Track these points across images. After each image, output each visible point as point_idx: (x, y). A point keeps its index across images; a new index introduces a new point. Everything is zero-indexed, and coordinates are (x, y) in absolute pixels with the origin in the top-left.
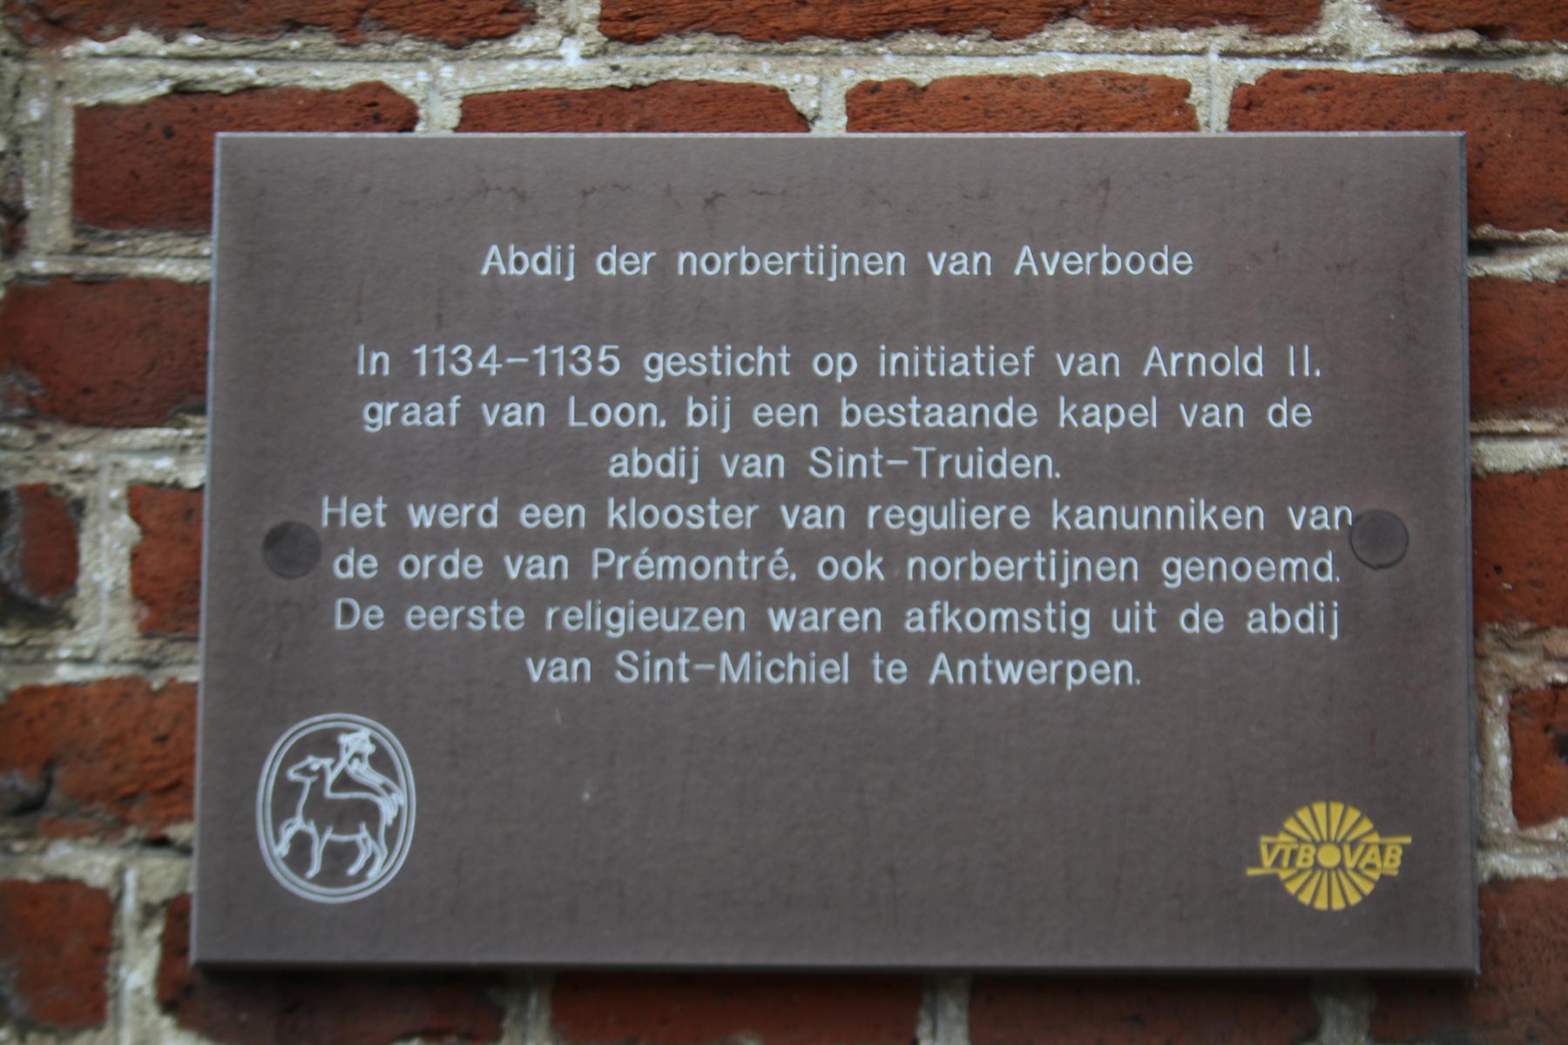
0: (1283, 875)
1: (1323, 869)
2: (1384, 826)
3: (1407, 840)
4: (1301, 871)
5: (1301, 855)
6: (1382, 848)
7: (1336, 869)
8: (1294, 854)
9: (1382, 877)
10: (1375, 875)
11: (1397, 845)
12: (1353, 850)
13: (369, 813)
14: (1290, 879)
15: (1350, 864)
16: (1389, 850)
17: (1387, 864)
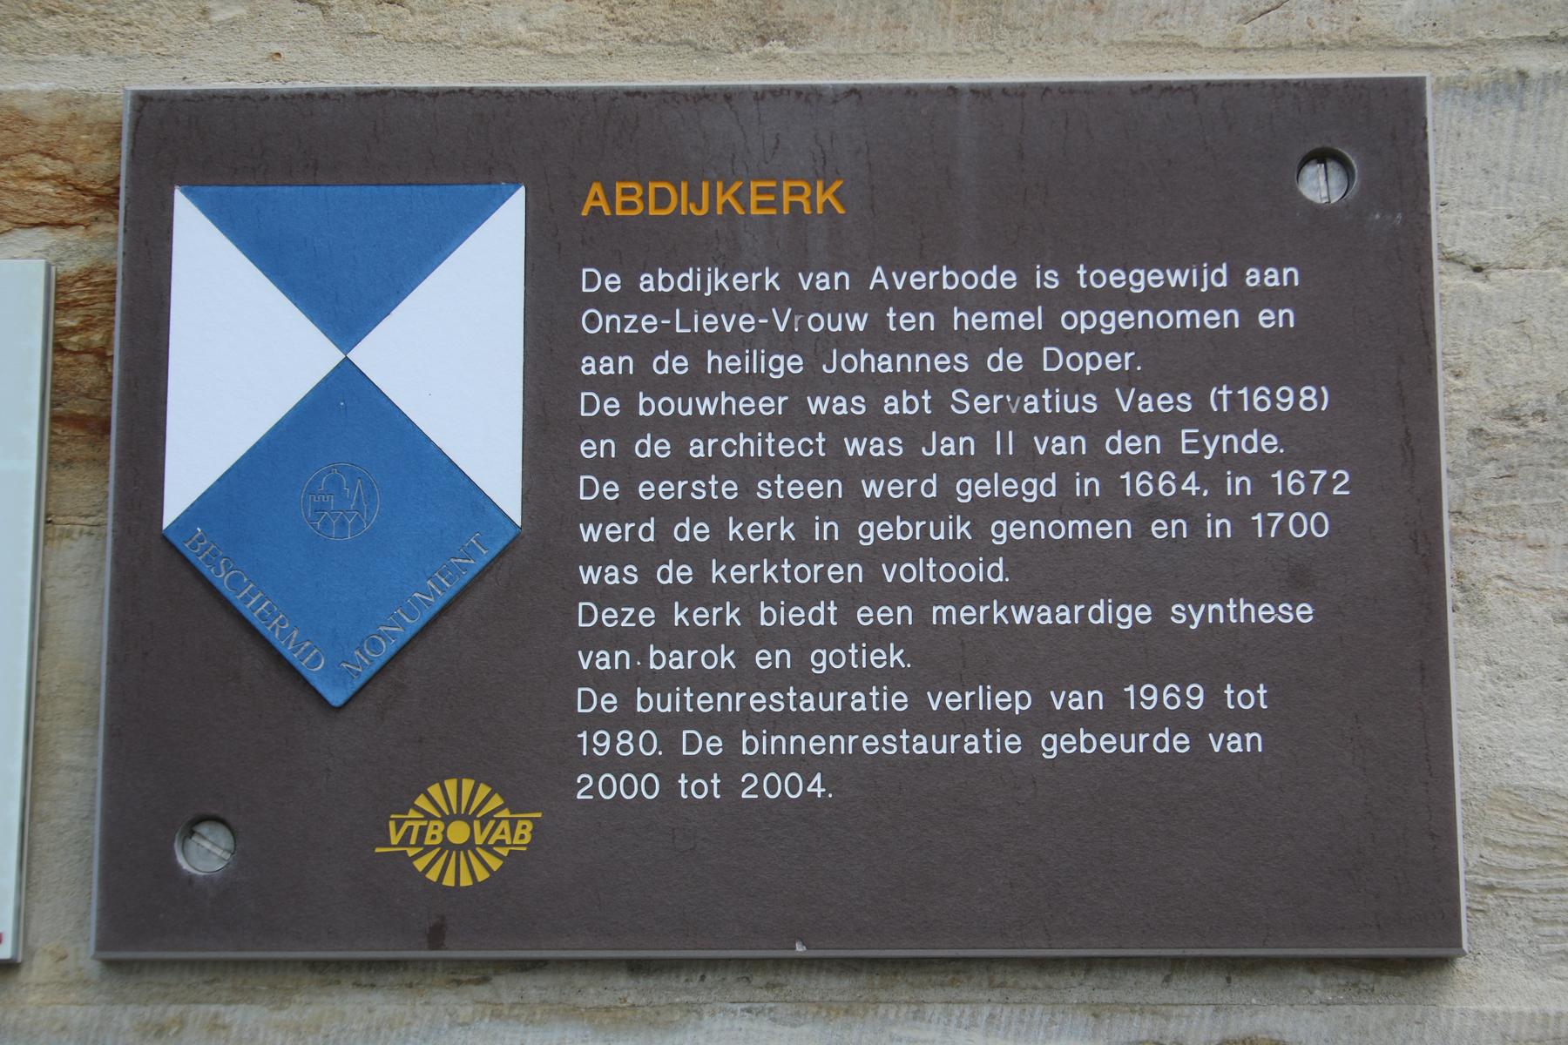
0: (411, 852)
4: (429, 848)
5: (430, 832)
6: (513, 823)
8: (423, 830)
10: (504, 852)
15: (479, 840)
16: (520, 823)
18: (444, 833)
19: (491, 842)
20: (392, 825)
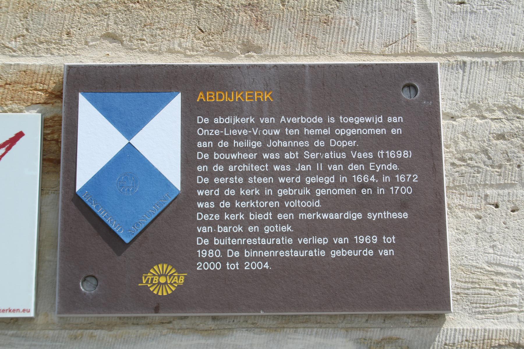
0: (149, 286)
2: (179, 271)
5: (154, 280)
6: (179, 277)
12: (170, 278)
14: (151, 287)
15: (169, 282)
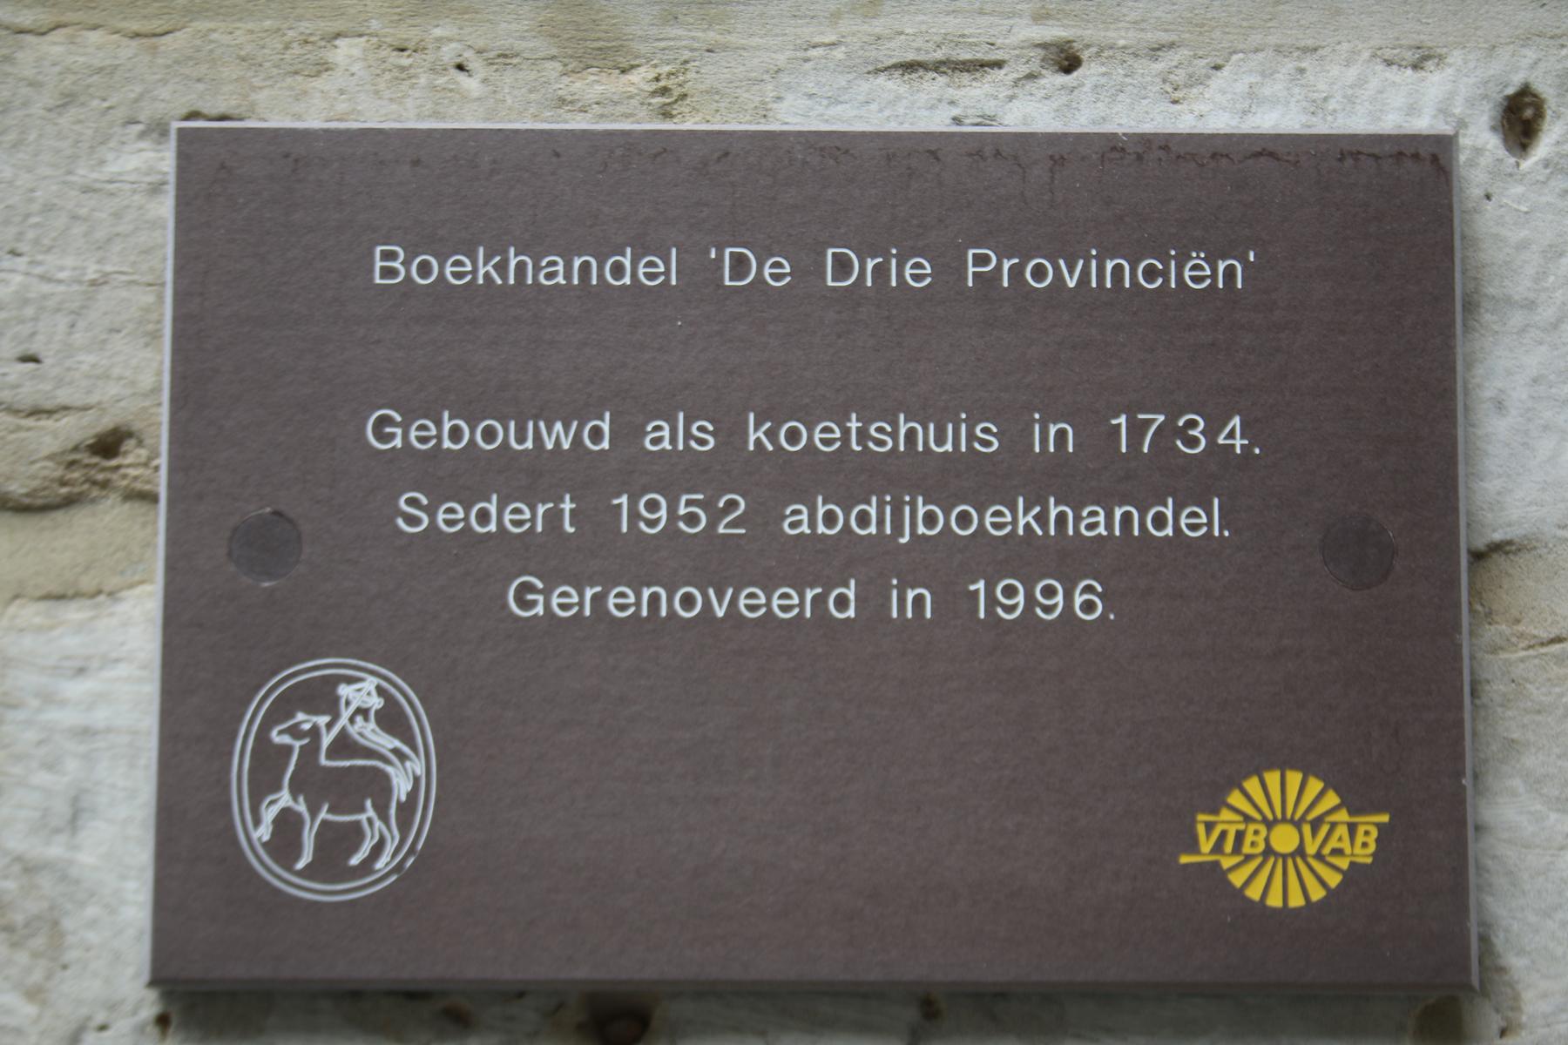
1: (1277, 855)
3: (1385, 818)
4: (1249, 858)
5: (1249, 838)
6: (1352, 828)
7: (1293, 855)
8: (1240, 836)
9: (1352, 864)
10: (1344, 864)
11: (1371, 825)
12: (1314, 832)
13: (379, 786)
15: (1311, 849)
16: (1361, 830)
17: (1358, 850)
18: (1267, 840)
19: (1326, 851)
20: (1201, 829)
